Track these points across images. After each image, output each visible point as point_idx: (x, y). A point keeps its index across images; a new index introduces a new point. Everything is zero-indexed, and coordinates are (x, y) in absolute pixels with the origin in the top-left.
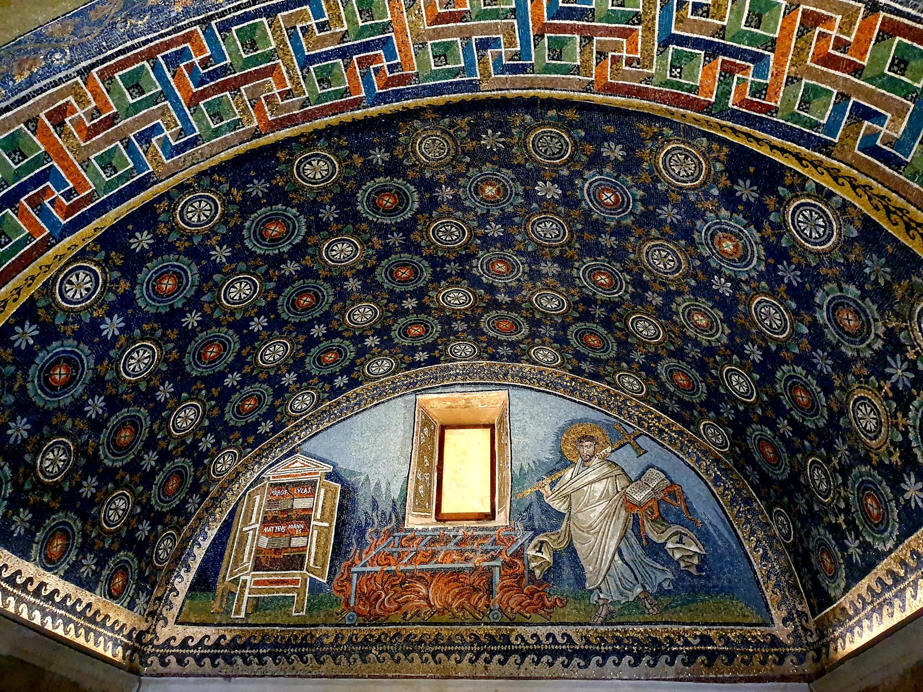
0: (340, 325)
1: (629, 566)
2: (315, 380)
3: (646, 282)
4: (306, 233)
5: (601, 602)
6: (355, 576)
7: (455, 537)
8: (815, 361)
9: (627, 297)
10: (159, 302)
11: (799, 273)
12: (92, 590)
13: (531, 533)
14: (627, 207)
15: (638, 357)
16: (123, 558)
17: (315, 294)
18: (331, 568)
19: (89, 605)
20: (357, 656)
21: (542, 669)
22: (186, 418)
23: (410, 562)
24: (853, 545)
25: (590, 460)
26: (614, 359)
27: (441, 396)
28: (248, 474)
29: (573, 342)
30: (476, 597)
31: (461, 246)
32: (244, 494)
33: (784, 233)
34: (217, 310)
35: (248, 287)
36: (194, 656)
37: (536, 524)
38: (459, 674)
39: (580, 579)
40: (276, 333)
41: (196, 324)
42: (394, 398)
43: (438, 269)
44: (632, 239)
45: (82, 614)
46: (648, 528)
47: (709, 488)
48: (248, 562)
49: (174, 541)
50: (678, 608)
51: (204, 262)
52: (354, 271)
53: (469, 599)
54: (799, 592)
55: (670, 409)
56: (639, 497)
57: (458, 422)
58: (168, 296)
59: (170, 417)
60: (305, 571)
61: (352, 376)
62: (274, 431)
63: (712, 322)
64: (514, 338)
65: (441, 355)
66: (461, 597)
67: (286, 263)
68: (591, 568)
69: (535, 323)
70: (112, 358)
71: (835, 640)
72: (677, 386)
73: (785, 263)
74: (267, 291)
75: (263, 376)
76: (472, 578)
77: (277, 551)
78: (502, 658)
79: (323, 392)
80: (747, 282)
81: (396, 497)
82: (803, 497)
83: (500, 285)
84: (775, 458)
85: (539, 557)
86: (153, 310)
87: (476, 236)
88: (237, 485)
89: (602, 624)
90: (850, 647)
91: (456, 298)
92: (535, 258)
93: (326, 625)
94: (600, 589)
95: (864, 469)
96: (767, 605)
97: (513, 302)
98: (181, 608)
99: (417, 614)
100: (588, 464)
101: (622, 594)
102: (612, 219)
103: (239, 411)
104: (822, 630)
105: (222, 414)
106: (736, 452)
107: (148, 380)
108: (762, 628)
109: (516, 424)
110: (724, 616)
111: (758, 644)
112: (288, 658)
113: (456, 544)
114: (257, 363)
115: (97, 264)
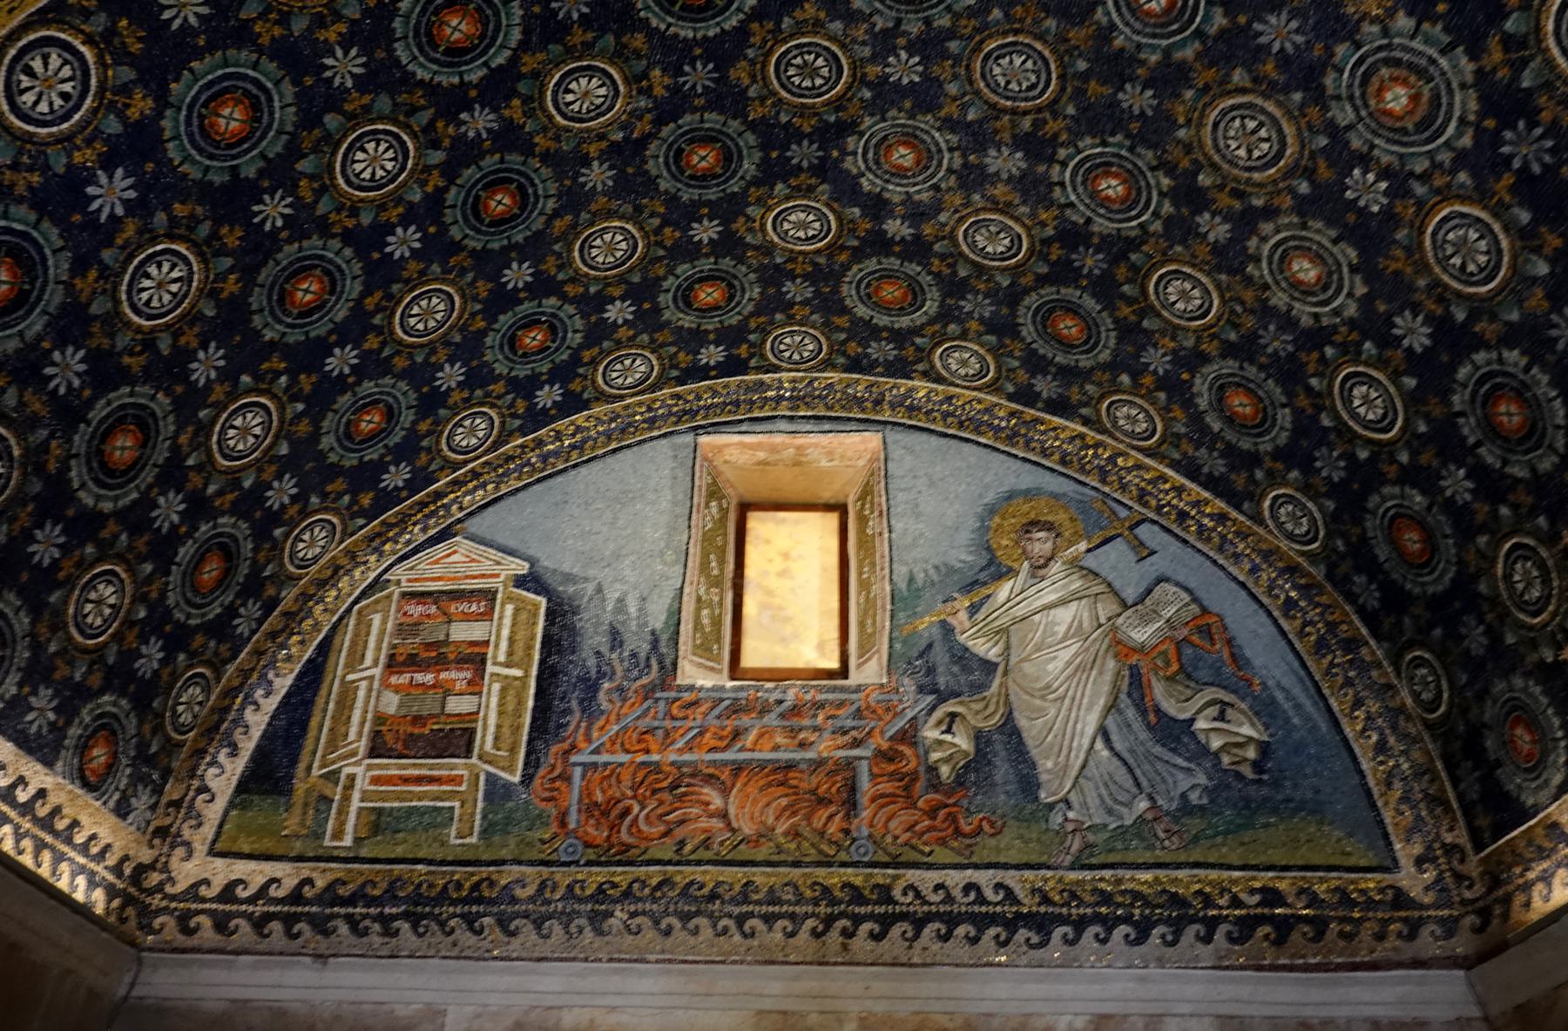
0: (560, 267)
1: (1126, 763)
2: (498, 388)
3: (1202, 191)
4: (521, 43)
5: (1070, 827)
6: (578, 771)
7: (780, 702)
8: (1554, 333)
9: (1157, 226)
10: (211, 157)
11: (1549, 144)
12: (49, 763)
13: (930, 698)
14: (1191, 20)
15: (1157, 360)
16: (109, 708)
17: (521, 187)
18: (528, 754)
19: (41, 794)
20: (583, 921)
21: (957, 948)
22: (245, 430)
23: (689, 747)
25: (1045, 566)
26: (1104, 367)
27: (747, 439)
28: (357, 573)
29: (1028, 331)
30: (823, 814)
31: (827, 103)
32: (349, 610)
33: (1532, 57)
34: (325, 199)
35: (390, 154)
36: (249, 916)
37: (942, 681)
38: (792, 958)
39: (1028, 783)
40: (436, 268)
41: (279, 223)
42: (652, 439)
43: (774, 155)
44: (1189, 94)
45: (26, 809)
47: (1275, 621)
48: (357, 735)
49: (207, 690)
50: (1219, 839)
51: (309, 81)
52: (604, 144)
53: (808, 818)
54: (1448, 808)
55: (1206, 470)
56: (1141, 635)
57: (776, 496)
58: (230, 146)
59: (213, 422)
60: (474, 760)
61: (572, 386)
62: (413, 486)
63: (1330, 274)
64: (904, 322)
65: (752, 356)
66: (794, 814)
67: (471, 110)
68: (1049, 764)
69: (954, 288)
70: (107, 267)
71: (1527, 887)
72: (1231, 420)
73: (1521, 124)
74: (427, 169)
75: (400, 363)
76: (814, 781)
77: (418, 720)
78: (877, 928)
79: (514, 416)
80: (1424, 177)
81: (659, 625)
82: (1481, 621)
83: (896, 199)
84: (1423, 551)
85: (947, 744)
86: (196, 174)
87: (864, 81)
88: (334, 593)
89: (1072, 868)
90: (1541, 906)
91: (799, 224)
92: (977, 137)
93: (520, 863)
94: (1066, 801)
96: (1386, 836)
97: (917, 237)
98: (221, 826)
99: (706, 844)
100: (1042, 572)
101: (1110, 812)
102: (1154, 48)
103: (348, 435)
104: (1495, 877)
105: (316, 436)
106: (1335, 550)
107: (175, 330)
108: (1378, 876)
109: (899, 498)
110: (1304, 855)
111: (1370, 904)
112: (442, 924)
113: (782, 716)
114: (392, 333)
115: (89, 40)
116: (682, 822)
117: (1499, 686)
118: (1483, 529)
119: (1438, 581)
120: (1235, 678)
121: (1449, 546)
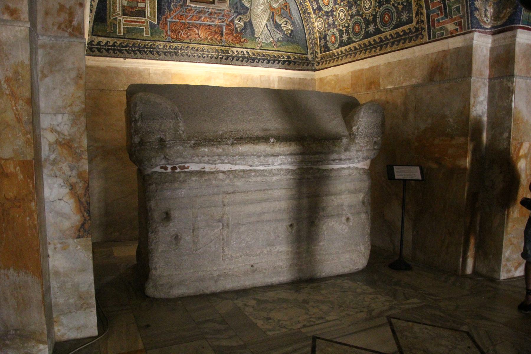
6: (169, 23)
23: (191, 19)
24: (345, 37)
30: (216, 37)
36: (105, 49)
37: (239, 11)
39: (253, 33)
46: (277, 18)
56: (275, 6)
77: (132, 8)
82: (333, 18)
85: (239, 24)
95: (359, 17)
99: (195, 40)
101: (266, 40)
112: (145, 52)
113: (208, 14)
116: (190, 35)
117: (332, 30)
118: (338, 4)
119: (328, 9)
120: (289, 17)
121: (331, 5)
